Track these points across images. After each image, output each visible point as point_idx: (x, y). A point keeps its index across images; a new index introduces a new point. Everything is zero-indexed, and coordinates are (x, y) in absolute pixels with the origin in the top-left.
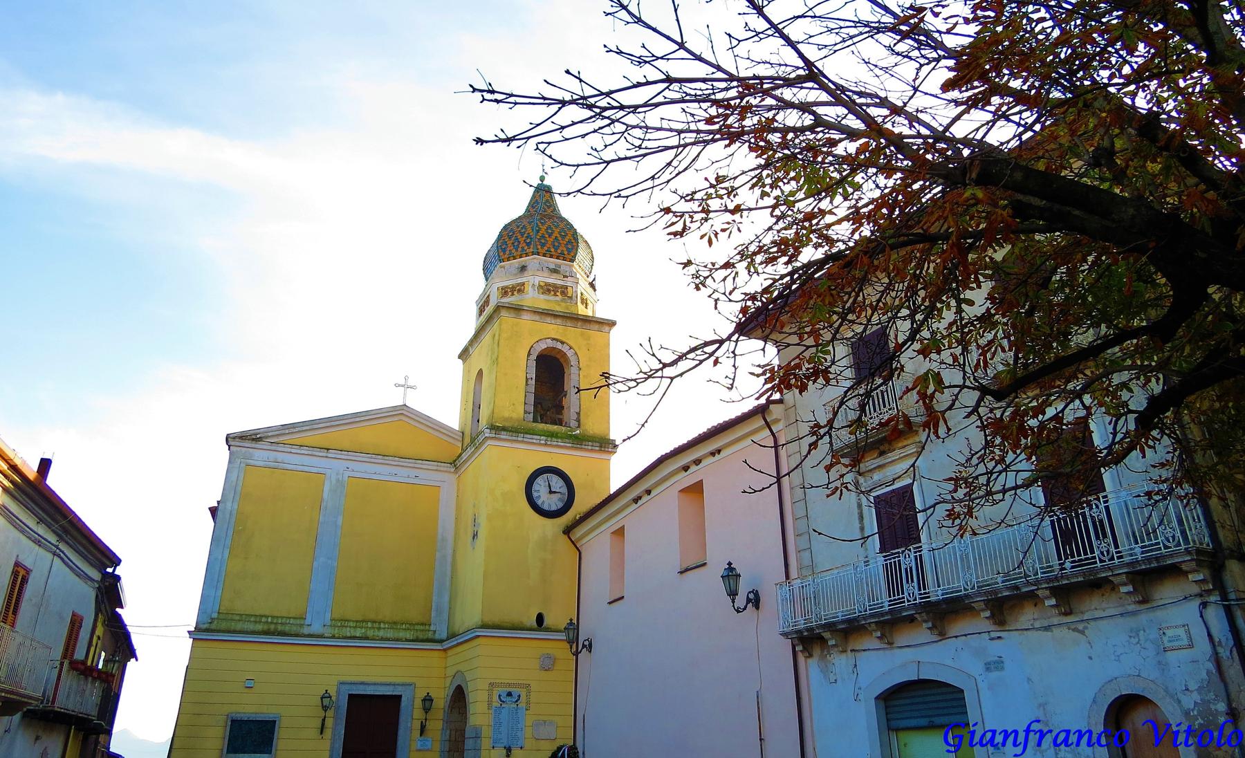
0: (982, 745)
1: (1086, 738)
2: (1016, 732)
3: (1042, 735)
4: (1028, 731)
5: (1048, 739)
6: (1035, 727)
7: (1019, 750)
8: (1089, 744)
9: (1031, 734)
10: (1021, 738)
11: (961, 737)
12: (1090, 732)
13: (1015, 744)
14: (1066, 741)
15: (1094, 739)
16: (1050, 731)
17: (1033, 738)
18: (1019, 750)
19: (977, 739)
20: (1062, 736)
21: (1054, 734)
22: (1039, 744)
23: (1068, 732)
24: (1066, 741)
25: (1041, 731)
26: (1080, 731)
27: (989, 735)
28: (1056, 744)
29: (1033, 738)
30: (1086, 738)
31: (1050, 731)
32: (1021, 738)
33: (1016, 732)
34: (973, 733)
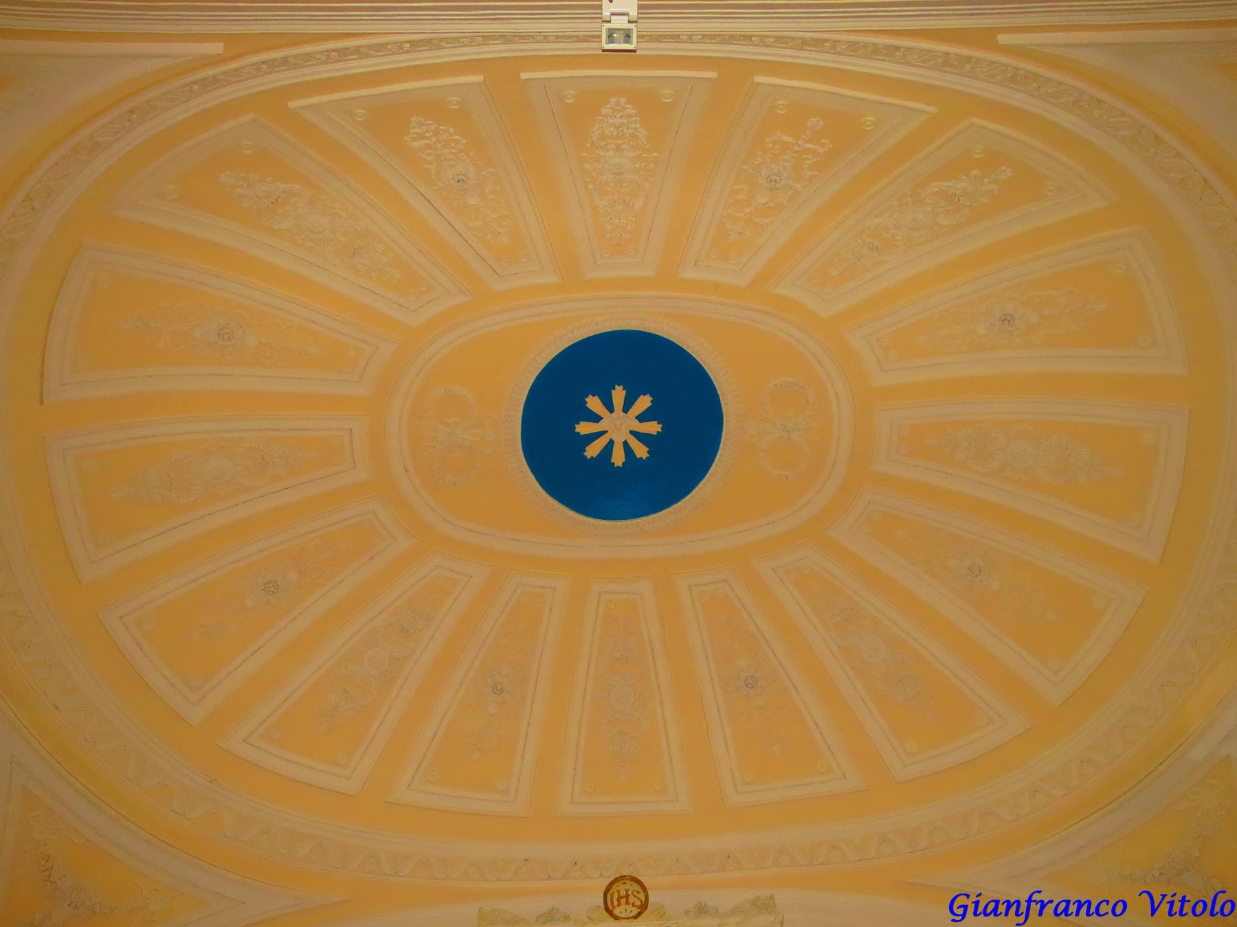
0: (986, 915)
1: (1085, 907)
2: (1018, 902)
3: (1043, 905)
4: (1029, 901)
5: (1049, 909)
6: (1036, 897)
7: (1021, 919)
8: (1088, 914)
9: (1033, 904)
10: (1023, 909)
11: (965, 907)
12: (1089, 902)
13: (1017, 914)
14: (1066, 911)
15: (1093, 910)
16: (1051, 901)
17: (1035, 908)
18: (1021, 919)
19: (980, 909)
20: (1063, 906)
21: (1054, 904)
22: (1040, 914)
23: (1068, 902)
24: (1066, 911)
25: (1042, 901)
26: (1079, 902)
27: (992, 905)
28: (1056, 914)
29: (1035, 908)
30: (1085, 907)
31: (1051, 901)
32: (1023, 909)
33: (1018, 902)
34: (977, 903)
